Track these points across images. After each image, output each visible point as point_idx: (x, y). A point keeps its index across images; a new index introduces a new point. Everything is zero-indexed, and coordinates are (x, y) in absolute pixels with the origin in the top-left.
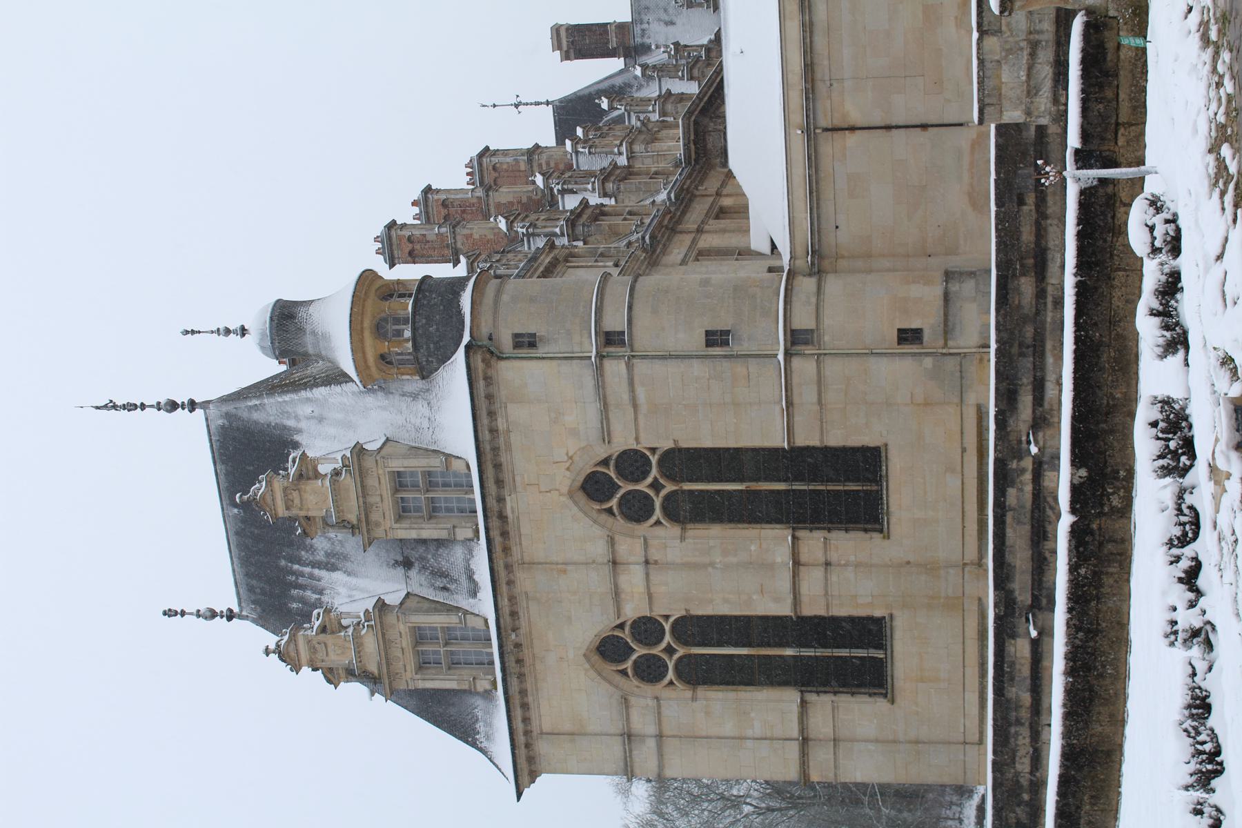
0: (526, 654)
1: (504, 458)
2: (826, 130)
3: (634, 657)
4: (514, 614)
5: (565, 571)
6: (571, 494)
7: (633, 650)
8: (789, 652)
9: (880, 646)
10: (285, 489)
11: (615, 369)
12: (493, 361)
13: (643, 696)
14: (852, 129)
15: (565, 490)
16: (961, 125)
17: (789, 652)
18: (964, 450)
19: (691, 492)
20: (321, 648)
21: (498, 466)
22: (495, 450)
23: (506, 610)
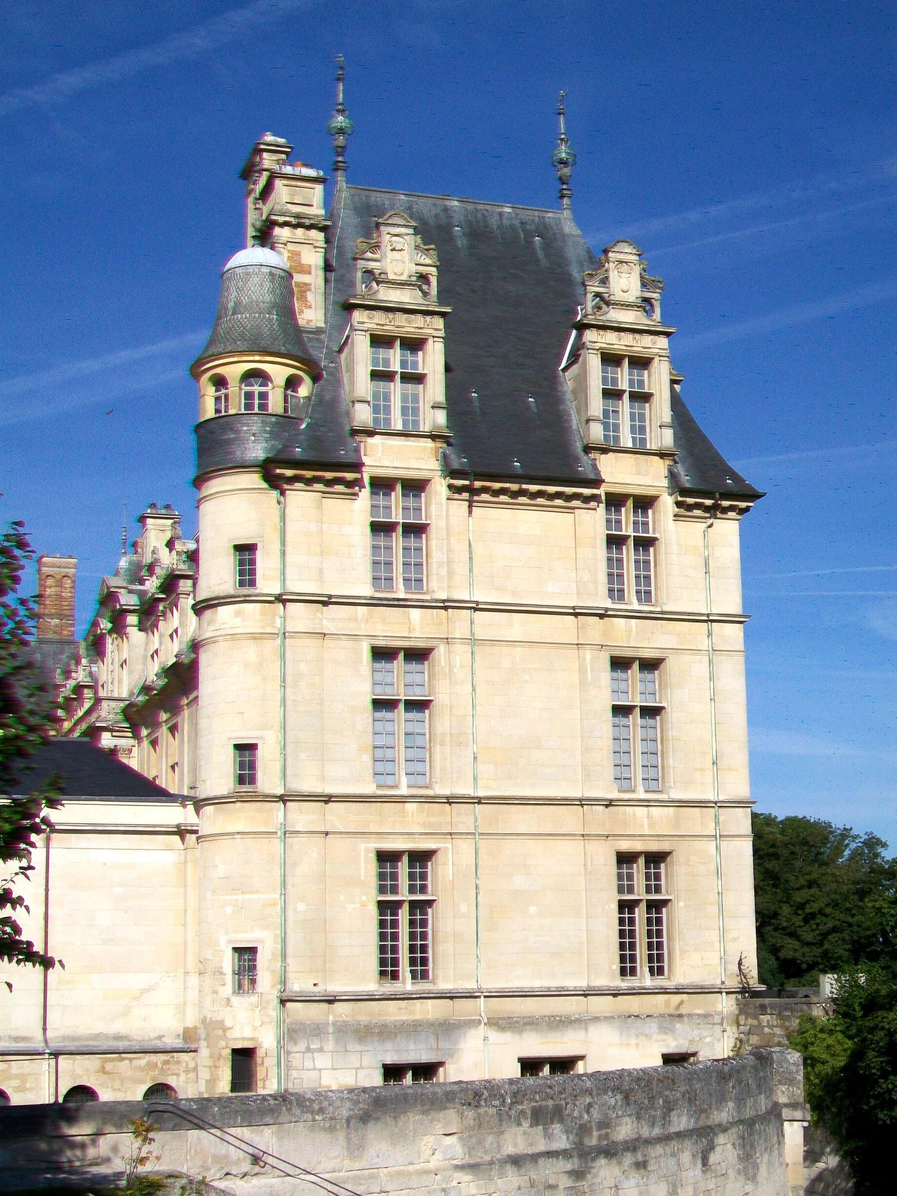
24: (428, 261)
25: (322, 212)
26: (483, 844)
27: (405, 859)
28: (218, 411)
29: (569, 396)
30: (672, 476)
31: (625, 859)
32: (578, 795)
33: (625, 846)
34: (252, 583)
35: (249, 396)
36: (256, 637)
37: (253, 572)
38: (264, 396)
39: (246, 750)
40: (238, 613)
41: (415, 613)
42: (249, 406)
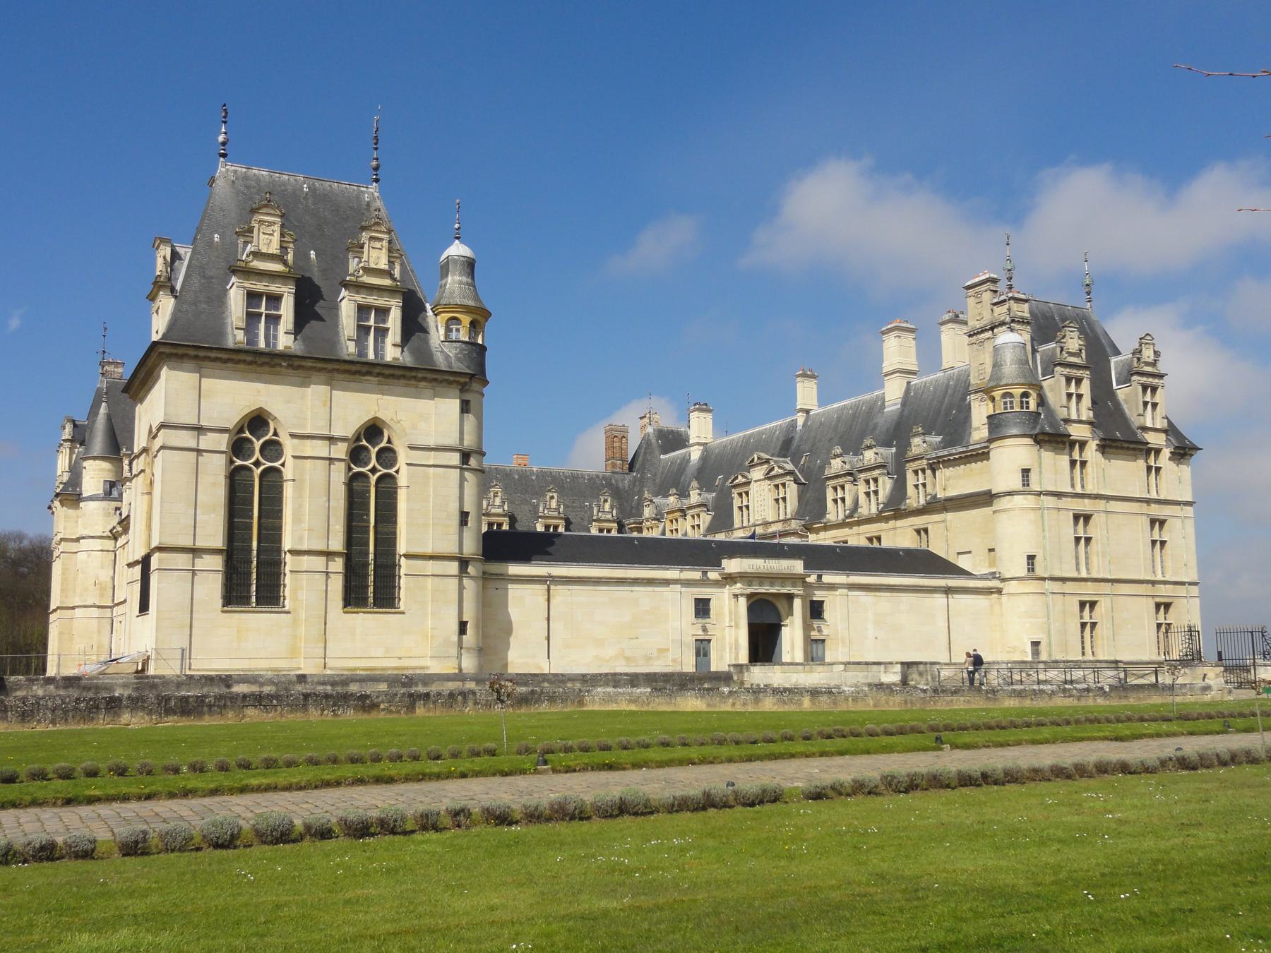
0: (267, 369)
1: (403, 381)
2: (549, 587)
3: (254, 439)
4: (300, 367)
5: (325, 405)
6: (376, 418)
7: (258, 440)
8: (255, 544)
9: (258, 603)
10: (381, 240)
11: (455, 458)
12: (460, 387)
13: (223, 442)
14: (549, 600)
15: (379, 415)
16: (549, 658)
17: (255, 544)
18: (400, 658)
19: (369, 492)
20: (269, 230)
21: (399, 377)
22: (410, 378)
23: (303, 363)
24: (1082, 343)
25: (1029, 315)
26: (1115, 598)
27: (1088, 605)
28: (1006, 408)
29: (1122, 403)
30: (1167, 440)
31: (1158, 606)
32: (1141, 578)
33: (1158, 600)
34: (1028, 485)
35: (1022, 402)
36: (1033, 509)
37: (1028, 480)
38: (1027, 403)
39: (1031, 558)
40: (1025, 499)
41: (1086, 501)
42: (1022, 408)
